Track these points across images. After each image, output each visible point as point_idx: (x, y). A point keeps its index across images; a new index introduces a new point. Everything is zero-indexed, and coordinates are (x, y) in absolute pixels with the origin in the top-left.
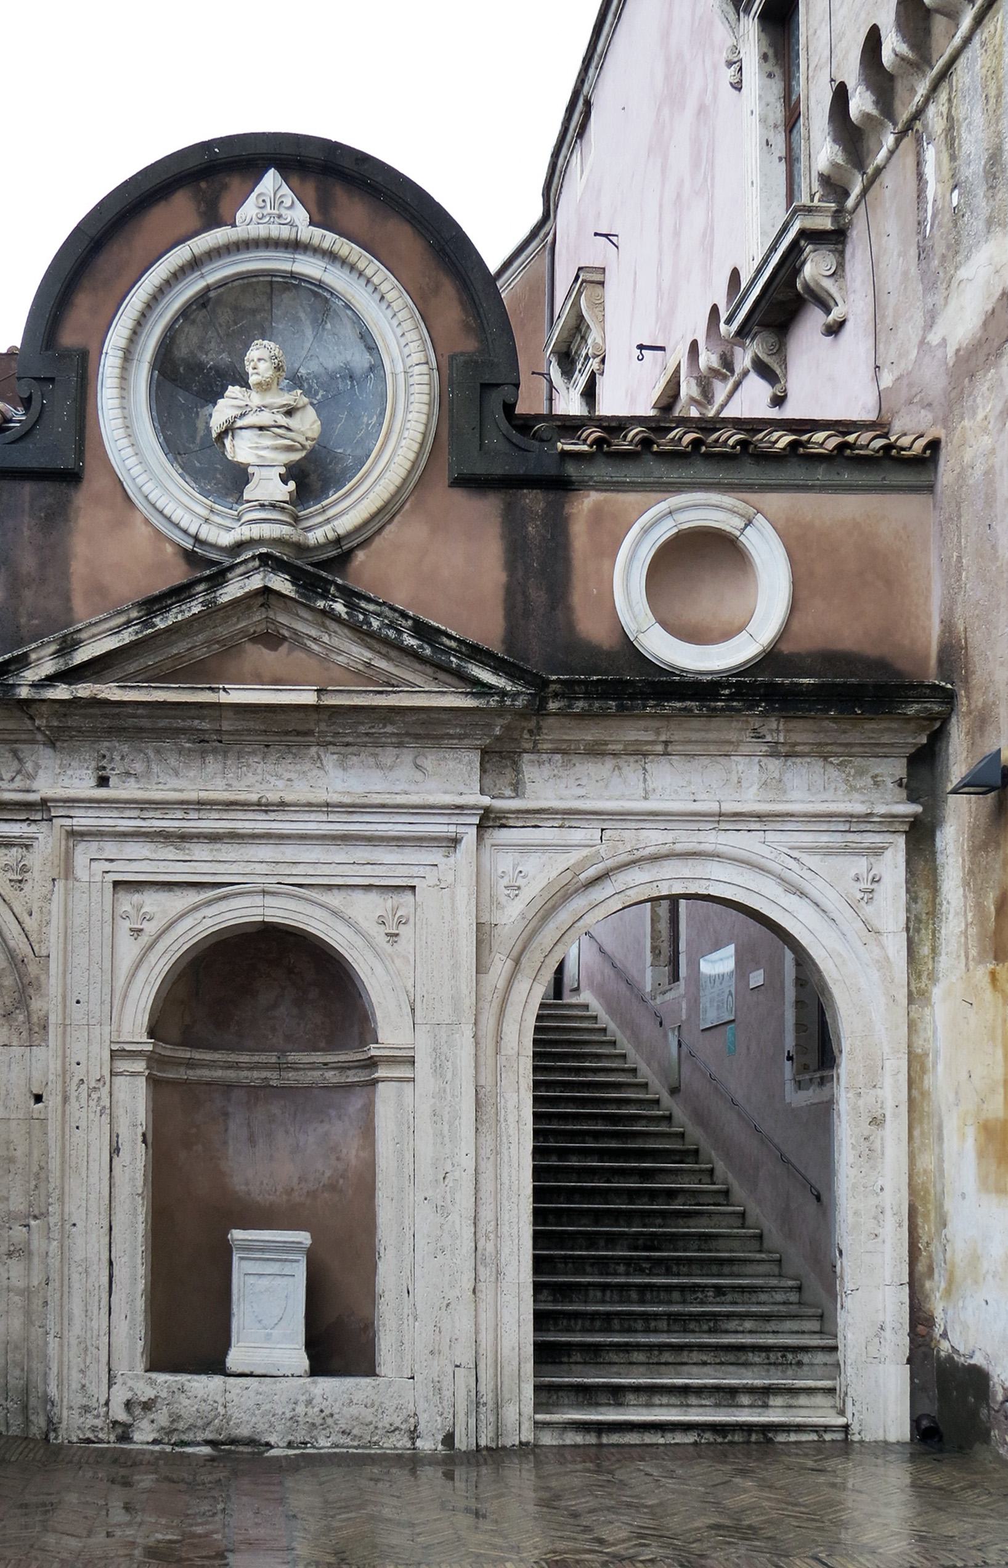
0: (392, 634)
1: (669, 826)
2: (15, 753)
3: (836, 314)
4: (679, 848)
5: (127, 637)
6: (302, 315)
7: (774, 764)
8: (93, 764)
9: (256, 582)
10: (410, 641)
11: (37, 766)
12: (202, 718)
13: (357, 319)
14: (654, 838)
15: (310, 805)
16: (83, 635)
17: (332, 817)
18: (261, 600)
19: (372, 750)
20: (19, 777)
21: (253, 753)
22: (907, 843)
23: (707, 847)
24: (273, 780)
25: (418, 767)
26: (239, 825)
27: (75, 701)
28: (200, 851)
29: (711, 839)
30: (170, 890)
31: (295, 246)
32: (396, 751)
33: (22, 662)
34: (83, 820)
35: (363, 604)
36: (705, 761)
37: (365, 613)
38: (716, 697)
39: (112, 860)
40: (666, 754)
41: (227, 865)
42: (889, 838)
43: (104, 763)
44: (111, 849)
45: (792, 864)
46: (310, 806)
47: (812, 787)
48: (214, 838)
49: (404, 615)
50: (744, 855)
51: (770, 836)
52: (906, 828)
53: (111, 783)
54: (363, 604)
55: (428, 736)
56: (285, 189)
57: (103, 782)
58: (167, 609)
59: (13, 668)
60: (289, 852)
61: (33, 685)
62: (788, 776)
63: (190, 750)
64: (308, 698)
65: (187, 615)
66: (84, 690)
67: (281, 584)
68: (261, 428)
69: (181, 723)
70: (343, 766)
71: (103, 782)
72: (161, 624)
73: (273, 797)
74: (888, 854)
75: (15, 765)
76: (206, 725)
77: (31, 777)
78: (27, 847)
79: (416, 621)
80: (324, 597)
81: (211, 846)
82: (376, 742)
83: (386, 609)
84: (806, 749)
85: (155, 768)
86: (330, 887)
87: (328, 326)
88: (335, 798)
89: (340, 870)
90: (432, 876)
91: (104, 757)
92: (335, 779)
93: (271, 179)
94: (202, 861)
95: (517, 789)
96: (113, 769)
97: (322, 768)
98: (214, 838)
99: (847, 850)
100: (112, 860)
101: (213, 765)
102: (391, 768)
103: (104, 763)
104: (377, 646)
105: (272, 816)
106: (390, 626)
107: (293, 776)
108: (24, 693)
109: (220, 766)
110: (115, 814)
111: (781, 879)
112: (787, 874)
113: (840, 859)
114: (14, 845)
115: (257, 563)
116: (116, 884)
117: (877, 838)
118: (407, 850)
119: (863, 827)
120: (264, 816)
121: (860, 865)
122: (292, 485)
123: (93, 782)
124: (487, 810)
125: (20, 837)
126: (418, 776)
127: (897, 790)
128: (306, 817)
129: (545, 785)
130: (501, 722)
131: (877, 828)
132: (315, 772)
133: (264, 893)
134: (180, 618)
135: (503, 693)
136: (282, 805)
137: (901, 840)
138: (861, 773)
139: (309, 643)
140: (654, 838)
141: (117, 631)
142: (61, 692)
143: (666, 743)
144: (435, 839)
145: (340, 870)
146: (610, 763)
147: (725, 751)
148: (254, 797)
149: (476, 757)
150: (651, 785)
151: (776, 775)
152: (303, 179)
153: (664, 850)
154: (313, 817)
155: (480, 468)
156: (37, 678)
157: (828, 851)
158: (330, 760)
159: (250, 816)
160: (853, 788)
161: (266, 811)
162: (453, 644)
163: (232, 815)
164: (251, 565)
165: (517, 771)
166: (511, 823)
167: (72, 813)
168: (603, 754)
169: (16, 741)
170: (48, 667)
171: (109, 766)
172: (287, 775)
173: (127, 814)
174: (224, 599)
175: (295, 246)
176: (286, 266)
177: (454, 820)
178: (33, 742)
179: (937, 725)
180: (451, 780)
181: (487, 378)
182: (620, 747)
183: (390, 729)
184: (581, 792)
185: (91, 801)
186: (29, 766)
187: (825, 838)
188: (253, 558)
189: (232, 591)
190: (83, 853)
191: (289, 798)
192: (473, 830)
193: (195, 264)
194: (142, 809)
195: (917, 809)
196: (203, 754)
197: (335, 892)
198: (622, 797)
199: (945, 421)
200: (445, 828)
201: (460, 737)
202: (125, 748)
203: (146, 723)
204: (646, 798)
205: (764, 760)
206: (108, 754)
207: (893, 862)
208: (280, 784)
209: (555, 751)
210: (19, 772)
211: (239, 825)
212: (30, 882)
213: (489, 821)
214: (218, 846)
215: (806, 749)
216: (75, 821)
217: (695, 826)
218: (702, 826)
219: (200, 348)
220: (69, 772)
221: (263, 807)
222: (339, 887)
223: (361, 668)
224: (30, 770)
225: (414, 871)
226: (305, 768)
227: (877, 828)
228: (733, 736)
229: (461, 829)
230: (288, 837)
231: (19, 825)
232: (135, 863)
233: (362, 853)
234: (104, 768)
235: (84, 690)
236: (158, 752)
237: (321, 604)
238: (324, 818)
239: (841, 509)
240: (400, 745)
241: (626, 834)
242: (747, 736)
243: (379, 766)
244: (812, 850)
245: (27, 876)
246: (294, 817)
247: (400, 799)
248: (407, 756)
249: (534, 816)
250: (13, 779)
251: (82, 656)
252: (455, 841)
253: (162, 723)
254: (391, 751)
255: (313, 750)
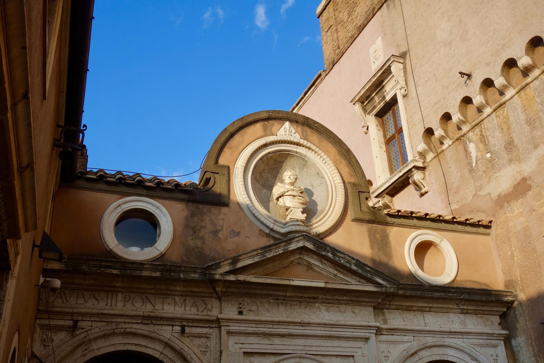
0: (348, 265)
1: (434, 336)
2: (204, 301)
3: (423, 191)
4: (438, 343)
5: (256, 259)
6: (296, 166)
7: (462, 316)
8: (237, 306)
9: (301, 244)
10: (354, 268)
11: (212, 307)
12: (280, 291)
13: (316, 168)
14: (430, 340)
15: (319, 324)
16: (241, 258)
17: (326, 329)
18: (299, 251)
19: (337, 305)
20: (205, 311)
21: (296, 305)
22: (505, 343)
23: (447, 344)
24: (304, 315)
25: (353, 312)
26: (293, 331)
27: (238, 282)
28: (277, 341)
29: (448, 341)
30: (264, 356)
31: (298, 144)
32: (345, 306)
33: (218, 265)
34: (234, 327)
35: (339, 254)
36: (441, 314)
37: (339, 257)
38: (450, 292)
39: (243, 344)
40: (430, 311)
41: (287, 346)
42: (499, 342)
43: (241, 306)
44: (242, 339)
45: (473, 350)
46: (319, 325)
47: (473, 324)
48: (283, 336)
49: (353, 258)
50: (458, 347)
51: (465, 340)
52: (503, 338)
53: (244, 313)
54: (339, 254)
55: (357, 301)
56: (292, 128)
57: (241, 313)
58: (271, 250)
59: (214, 267)
60: (310, 342)
61: (221, 274)
62: (467, 320)
63: (273, 302)
64: (322, 285)
65: (278, 253)
66: (241, 277)
67: (309, 245)
68: (294, 196)
69: (271, 293)
70: (327, 310)
71: (241, 313)
72: (269, 255)
73: (306, 321)
74: (499, 347)
75: (204, 306)
76: (281, 294)
77: (211, 311)
78: (208, 338)
79: (357, 260)
80: (324, 251)
81: (281, 339)
82: (339, 302)
83: (347, 257)
84: (472, 311)
85: (260, 309)
86: (324, 355)
87: (305, 170)
88: (328, 322)
89: (328, 349)
90: (360, 352)
91: (241, 304)
92: (324, 315)
93: (287, 124)
94: (278, 345)
95: (385, 322)
96: (244, 308)
97: (320, 311)
98: (283, 336)
99: (487, 345)
100: (243, 344)
101: (282, 308)
102: (344, 312)
103: (241, 306)
104: (340, 269)
105: (304, 328)
106: (347, 262)
107: (311, 314)
108: (217, 277)
109: (284, 309)
110: (246, 325)
111: (470, 355)
112: (471, 353)
113: (485, 348)
114: (203, 337)
115: (302, 238)
116: (244, 353)
117: (496, 342)
118: (351, 342)
119: (492, 338)
120: (301, 328)
121: (492, 351)
122: (305, 215)
123: (237, 313)
124: (378, 327)
125: (206, 334)
126: (354, 315)
127: (499, 326)
128: (316, 328)
129: (396, 319)
130: (382, 297)
131: (495, 338)
132: (318, 312)
133: (300, 357)
134: (275, 254)
135: (386, 287)
136: (309, 324)
137: (502, 342)
138: (487, 320)
139: (314, 267)
140: (430, 340)
141: (254, 256)
142: (232, 278)
143: (431, 307)
144: (361, 338)
145: (328, 349)
146: (412, 313)
147: (447, 311)
148: (299, 320)
149: (372, 309)
150: (427, 321)
151: (463, 319)
152: (297, 126)
153: (433, 344)
154: (319, 329)
155: (361, 216)
156: (223, 272)
157: (482, 346)
158: (323, 308)
159: (297, 327)
160: (486, 325)
161: (302, 326)
162: (369, 269)
163: (290, 327)
164: (300, 238)
165: (383, 314)
166: (384, 333)
167: (229, 324)
168: (410, 310)
169: (204, 297)
170: (227, 268)
171: (243, 307)
172: (308, 313)
173: (251, 325)
174: (291, 249)
175: (298, 144)
176: (295, 150)
177: (368, 331)
178: (212, 297)
179: (510, 305)
180: (364, 316)
181: (360, 190)
182: (416, 308)
183: (345, 298)
184: (405, 323)
185: (237, 320)
186: (209, 306)
187: (481, 341)
188: (301, 236)
189: (293, 246)
190: (232, 340)
191: (312, 321)
192: (374, 335)
193: (265, 145)
194: (257, 324)
195: (508, 332)
196: (278, 305)
197: (325, 357)
198: (418, 325)
199: (494, 216)
200: (364, 334)
201: (367, 302)
202: (249, 301)
203: (258, 292)
204: (425, 326)
205: (459, 315)
206: (242, 303)
207: (501, 350)
208: (306, 316)
209: (395, 309)
210: (205, 308)
211: (293, 331)
212: (209, 352)
213: (379, 331)
214: (283, 339)
215: (472, 311)
216: (230, 328)
217: (442, 336)
218: (444, 336)
219: (263, 171)
220: (228, 309)
221: (302, 324)
222: (327, 355)
223: (332, 277)
224: (210, 307)
225: (354, 350)
226: (315, 311)
227: (495, 338)
228: (451, 306)
229: (370, 335)
230: (309, 336)
231: (205, 329)
232: (252, 345)
233: (336, 343)
234: (240, 308)
235: (241, 277)
236: (261, 303)
237: (323, 253)
238: (323, 329)
239: (468, 238)
240: (347, 304)
241: (422, 338)
242: (455, 306)
243: (340, 311)
244: (478, 345)
245: (208, 349)
246: (312, 328)
247: (350, 323)
248: (349, 308)
249: (393, 331)
250: (203, 311)
251: (240, 265)
252: (367, 339)
253: (265, 292)
254: (343, 306)
255: (317, 305)
